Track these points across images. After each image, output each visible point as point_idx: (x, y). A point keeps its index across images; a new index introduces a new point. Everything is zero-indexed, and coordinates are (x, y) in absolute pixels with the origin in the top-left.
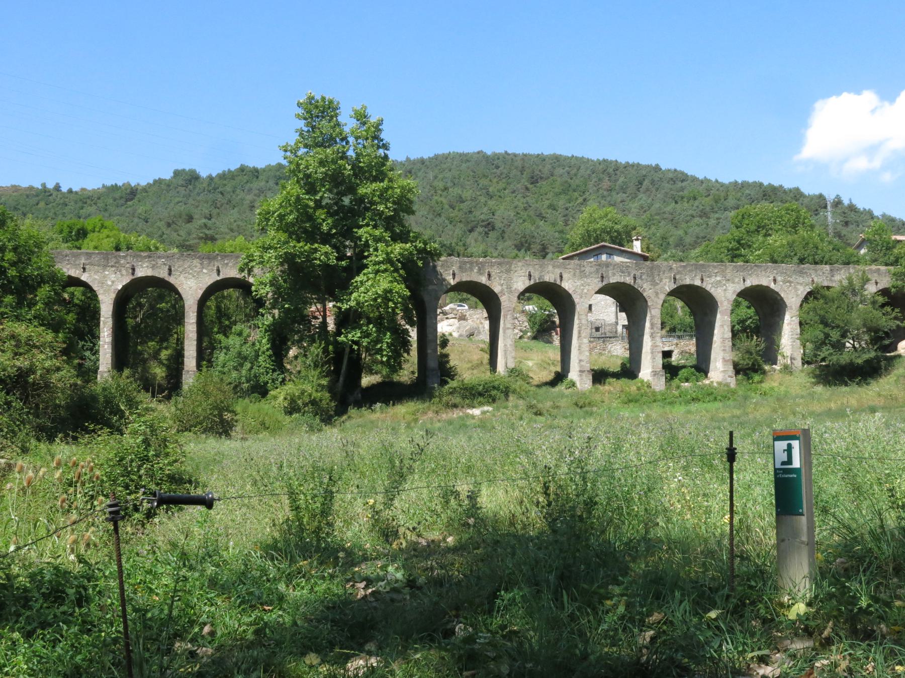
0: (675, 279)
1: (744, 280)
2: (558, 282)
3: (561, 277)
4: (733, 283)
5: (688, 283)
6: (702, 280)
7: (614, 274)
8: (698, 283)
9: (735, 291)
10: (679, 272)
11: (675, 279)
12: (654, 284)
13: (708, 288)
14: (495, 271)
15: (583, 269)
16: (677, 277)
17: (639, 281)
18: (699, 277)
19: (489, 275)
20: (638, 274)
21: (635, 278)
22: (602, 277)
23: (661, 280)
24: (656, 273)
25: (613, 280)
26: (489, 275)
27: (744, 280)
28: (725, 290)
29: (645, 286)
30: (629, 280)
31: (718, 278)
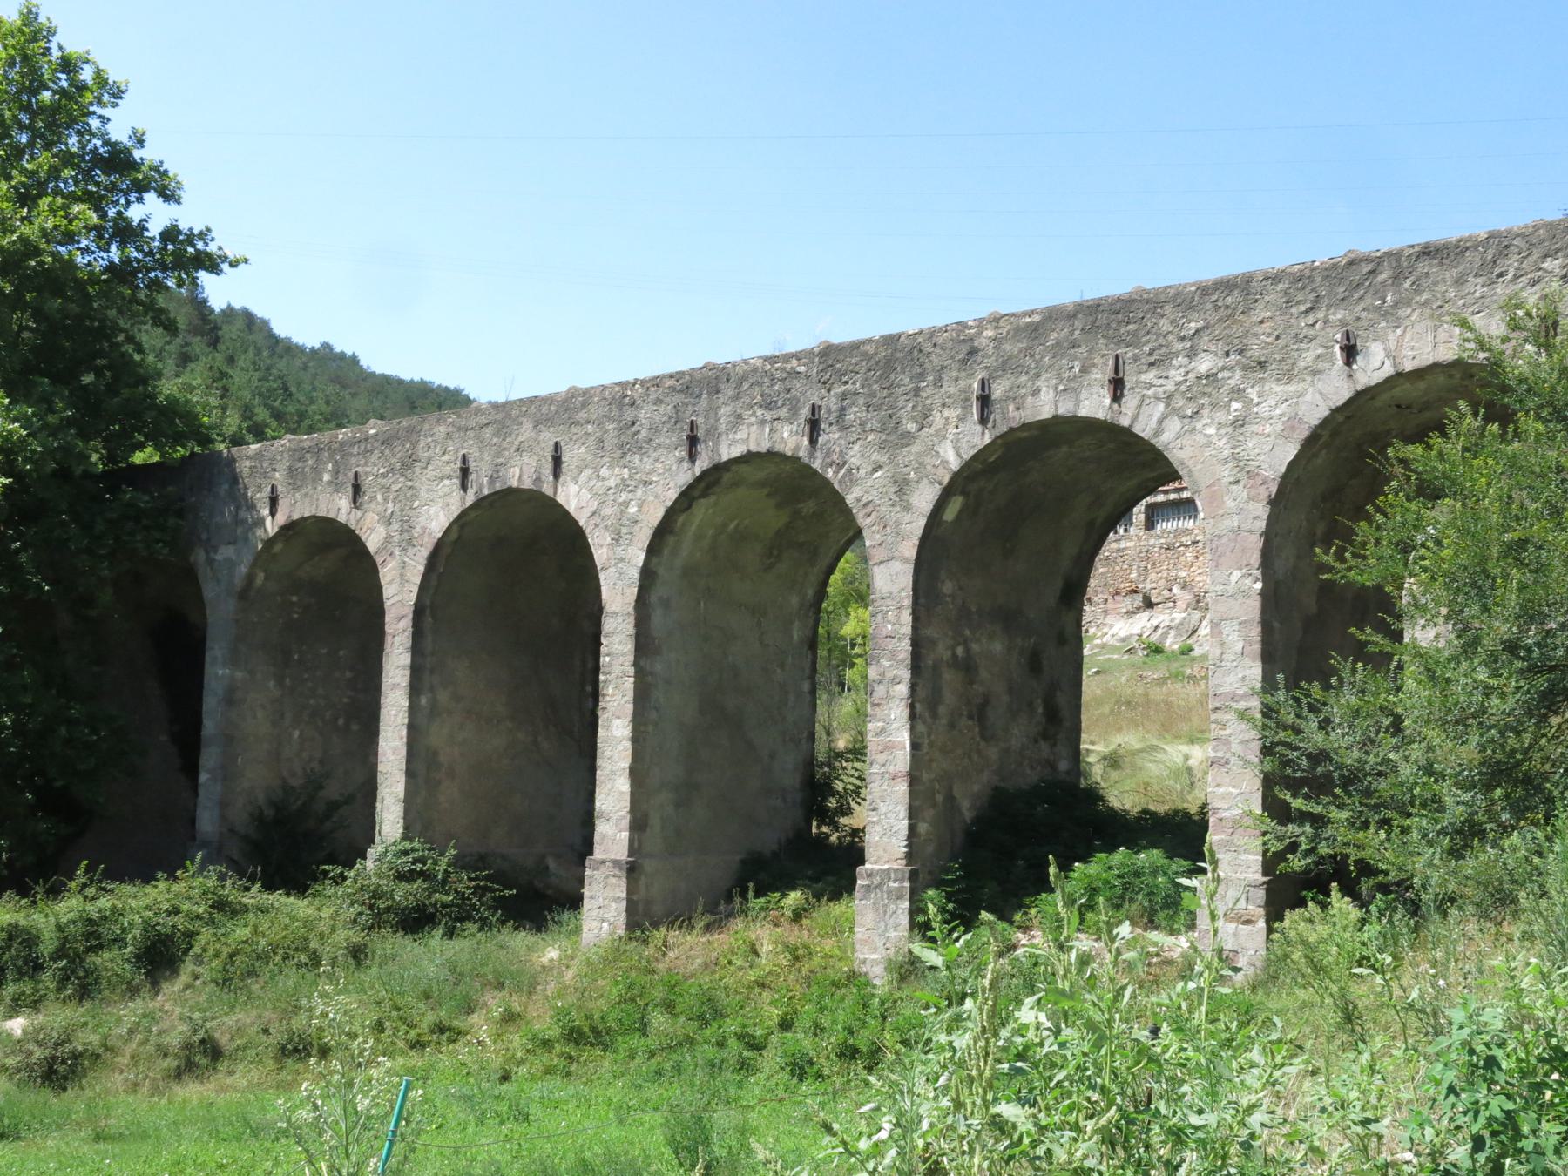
0: (985, 400)
1: (1350, 352)
2: (547, 489)
3: (557, 461)
4: (1288, 376)
5: (1046, 413)
6: (1117, 386)
7: (738, 419)
8: (1094, 404)
9: (1292, 421)
10: (1007, 366)
11: (985, 400)
12: (894, 438)
13: (1144, 429)
14: (372, 469)
15: (629, 415)
16: (997, 392)
17: (830, 436)
18: (1101, 374)
19: (357, 490)
20: (831, 403)
21: (814, 426)
22: (693, 441)
23: (924, 419)
24: (905, 381)
25: (729, 450)
26: (357, 490)
27: (1350, 352)
28: (1239, 423)
29: (855, 457)
30: (790, 439)
31: (1204, 364)
